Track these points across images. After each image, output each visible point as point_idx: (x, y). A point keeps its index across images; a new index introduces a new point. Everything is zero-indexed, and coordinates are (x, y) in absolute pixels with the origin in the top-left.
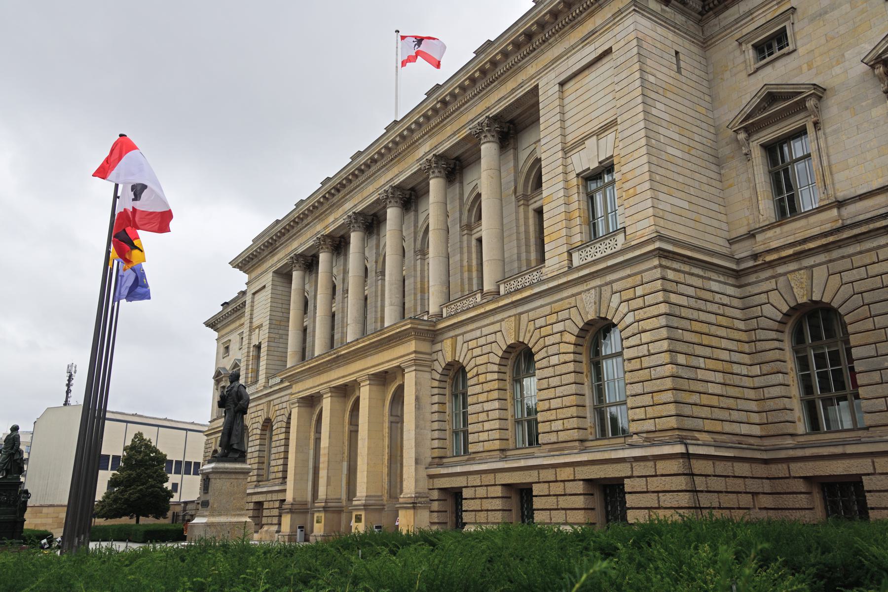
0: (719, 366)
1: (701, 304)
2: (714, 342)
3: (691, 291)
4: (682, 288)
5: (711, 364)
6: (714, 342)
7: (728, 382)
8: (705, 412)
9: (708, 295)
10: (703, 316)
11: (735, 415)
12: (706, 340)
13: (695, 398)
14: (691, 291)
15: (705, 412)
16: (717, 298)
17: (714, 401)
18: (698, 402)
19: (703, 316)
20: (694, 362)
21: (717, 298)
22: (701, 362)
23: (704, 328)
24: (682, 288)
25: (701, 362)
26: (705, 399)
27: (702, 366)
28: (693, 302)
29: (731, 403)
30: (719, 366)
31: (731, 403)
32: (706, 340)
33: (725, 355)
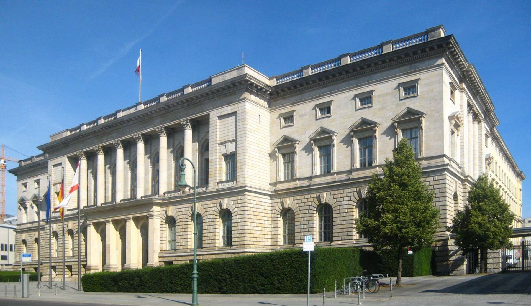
0: (260, 225)
1: (258, 206)
2: (260, 218)
3: (255, 202)
4: (252, 202)
5: (258, 225)
6: (260, 218)
7: (262, 230)
8: (255, 239)
9: (260, 203)
10: (258, 210)
11: (264, 240)
12: (258, 217)
13: (252, 235)
14: (255, 202)
15: (255, 239)
16: (263, 204)
17: (257, 236)
18: (253, 236)
19: (258, 210)
20: (253, 224)
21: (263, 204)
22: (255, 225)
23: (257, 214)
24: (252, 202)
25: (255, 225)
26: (255, 236)
27: (255, 226)
28: (255, 206)
29: (263, 236)
30: (260, 225)
31: (263, 236)
32: (258, 217)
33: (263, 222)
